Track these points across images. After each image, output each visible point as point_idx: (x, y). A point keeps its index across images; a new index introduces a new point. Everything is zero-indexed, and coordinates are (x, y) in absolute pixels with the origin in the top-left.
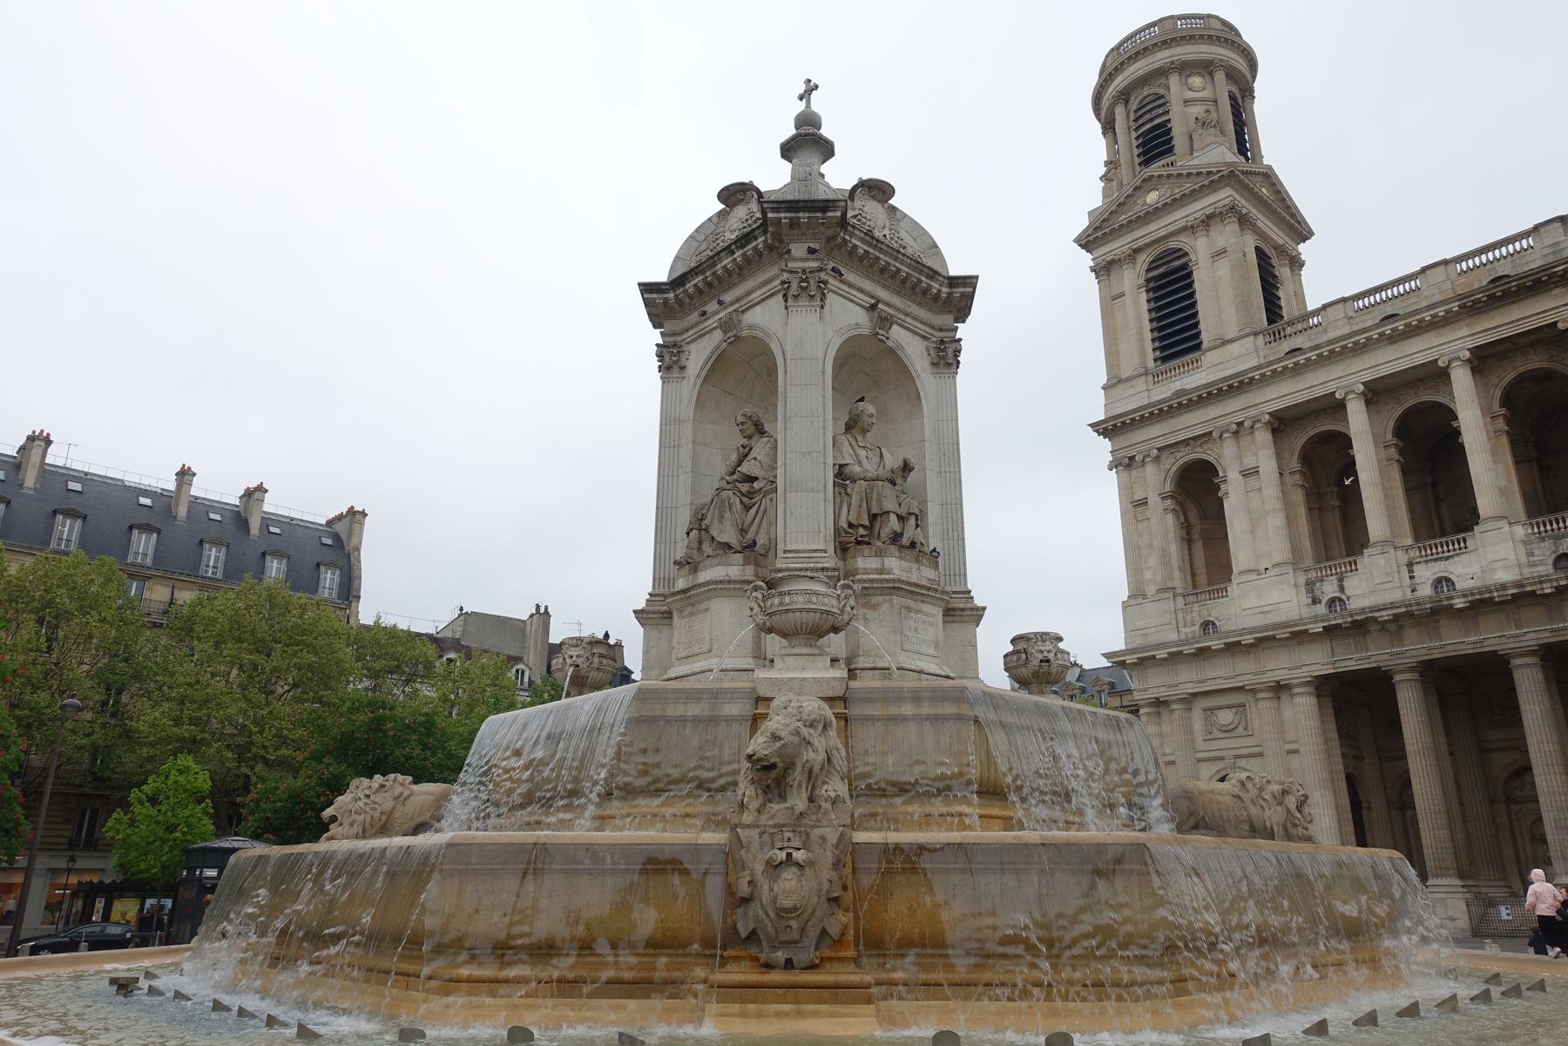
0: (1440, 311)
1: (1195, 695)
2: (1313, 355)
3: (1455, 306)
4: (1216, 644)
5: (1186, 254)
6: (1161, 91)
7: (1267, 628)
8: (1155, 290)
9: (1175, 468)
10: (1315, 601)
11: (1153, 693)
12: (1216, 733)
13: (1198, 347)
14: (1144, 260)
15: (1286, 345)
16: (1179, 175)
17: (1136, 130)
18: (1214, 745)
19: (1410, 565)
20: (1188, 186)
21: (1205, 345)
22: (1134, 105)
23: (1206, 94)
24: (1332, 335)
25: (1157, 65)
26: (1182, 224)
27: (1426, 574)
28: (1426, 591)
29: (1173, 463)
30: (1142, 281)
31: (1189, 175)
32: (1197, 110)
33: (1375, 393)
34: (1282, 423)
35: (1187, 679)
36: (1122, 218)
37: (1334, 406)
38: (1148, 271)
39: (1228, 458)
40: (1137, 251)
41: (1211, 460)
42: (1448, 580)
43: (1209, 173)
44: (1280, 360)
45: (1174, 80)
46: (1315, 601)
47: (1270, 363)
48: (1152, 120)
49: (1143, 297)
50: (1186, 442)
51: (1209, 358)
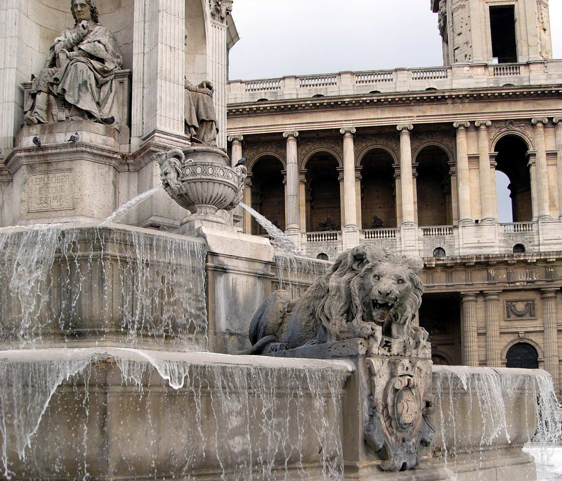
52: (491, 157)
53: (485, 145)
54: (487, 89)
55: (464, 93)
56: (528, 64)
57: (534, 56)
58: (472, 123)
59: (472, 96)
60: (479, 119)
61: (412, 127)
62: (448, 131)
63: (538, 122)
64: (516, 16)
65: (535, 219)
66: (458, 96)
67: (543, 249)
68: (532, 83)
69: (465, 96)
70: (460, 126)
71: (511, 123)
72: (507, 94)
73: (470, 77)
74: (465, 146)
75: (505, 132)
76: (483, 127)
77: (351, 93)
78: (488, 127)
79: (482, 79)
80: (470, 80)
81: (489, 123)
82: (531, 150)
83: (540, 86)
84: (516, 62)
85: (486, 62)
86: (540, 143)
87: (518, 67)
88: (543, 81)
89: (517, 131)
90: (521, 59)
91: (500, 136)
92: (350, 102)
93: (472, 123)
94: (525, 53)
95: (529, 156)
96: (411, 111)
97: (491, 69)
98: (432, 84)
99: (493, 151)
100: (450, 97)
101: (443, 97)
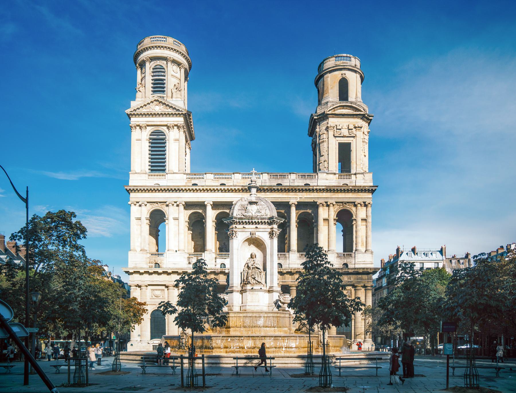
0: (237, 188)
1: (149, 285)
2: (201, 188)
3: (240, 188)
4: (160, 271)
5: (165, 135)
6: (165, 67)
7: (176, 269)
8: (152, 143)
9: (151, 210)
10: (189, 263)
11: (136, 283)
12: (154, 297)
13: (164, 170)
14: (150, 130)
15: (194, 182)
16: (168, 105)
17: (153, 76)
18: (153, 300)
19: (216, 258)
20: (170, 111)
21: (167, 171)
22: (153, 67)
23: (178, 75)
24: (207, 184)
25: (165, 55)
26: (165, 123)
27: (220, 261)
28: (218, 266)
29: (150, 208)
30: (148, 138)
31: (171, 107)
32: (176, 81)
33: (216, 205)
34: (188, 205)
35: (147, 279)
36: (144, 110)
37: (202, 205)
38: (150, 135)
39: (171, 212)
40: (148, 126)
41: (164, 211)
42: (224, 264)
43: (178, 110)
44: (191, 186)
45: (169, 63)
46: (189, 263)
47: (189, 186)
48: (159, 76)
49: (148, 144)
50: (157, 202)
51: (169, 176)
52: (334, 220)
53: (333, 213)
54: (334, 186)
55: (323, 188)
56: (355, 174)
57: (359, 170)
58: (326, 202)
59: (327, 189)
60: (330, 201)
61: (297, 203)
62: (314, 206)
63: (359, 204)
64: (352, 149)
65: (354, 251)
66: (320, 189)
67: (357, 266)
68: (358, 184)
69: (323, 189)
70: (320, 204)
71: (346, 204)
72: (344, 189)
73: (327, 179)
74: (323, 213)
75: (342, 207)
76: (331, 205)
77: (268, 184)
78: (333, 205)
79: (333, 181)
80: (327, 181)
81: (335, 203)
82: (354, 217)
83: (360, 187)
84: (350, 172)
85: (335, 172)
86: (361, 213)
87: (350, 175)
88: (362, 184)
89: (348, 207)
90: (353, 171)
91: (339, 210)
92: (267, 189)
93: (326, 202)
94: (355, 168)
95: (353, 220)
96: (297, 195)
97: (337, 175)
98: (308, 182)
99: (335, 217)
100: (316, 189)
101: (313, 189)
